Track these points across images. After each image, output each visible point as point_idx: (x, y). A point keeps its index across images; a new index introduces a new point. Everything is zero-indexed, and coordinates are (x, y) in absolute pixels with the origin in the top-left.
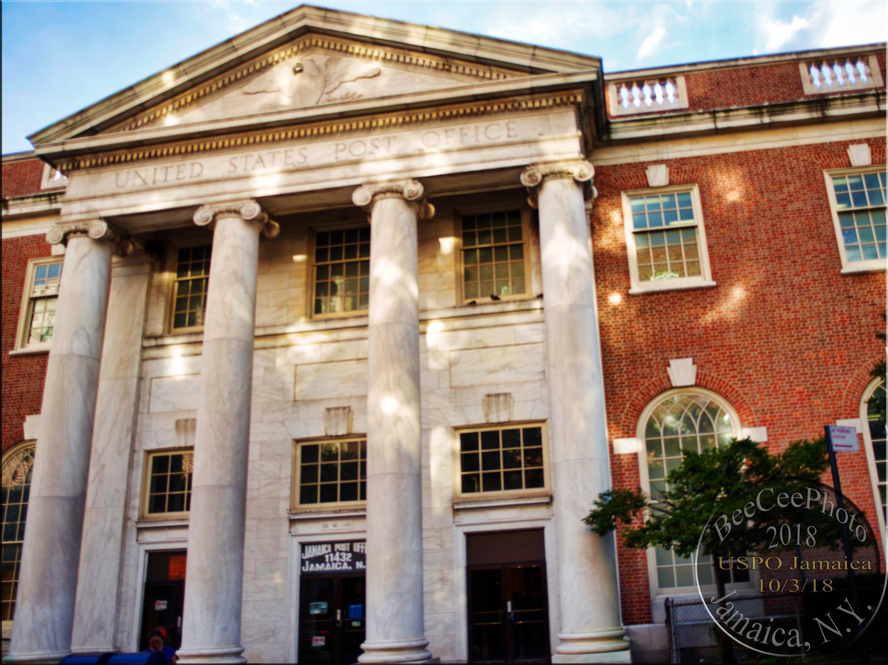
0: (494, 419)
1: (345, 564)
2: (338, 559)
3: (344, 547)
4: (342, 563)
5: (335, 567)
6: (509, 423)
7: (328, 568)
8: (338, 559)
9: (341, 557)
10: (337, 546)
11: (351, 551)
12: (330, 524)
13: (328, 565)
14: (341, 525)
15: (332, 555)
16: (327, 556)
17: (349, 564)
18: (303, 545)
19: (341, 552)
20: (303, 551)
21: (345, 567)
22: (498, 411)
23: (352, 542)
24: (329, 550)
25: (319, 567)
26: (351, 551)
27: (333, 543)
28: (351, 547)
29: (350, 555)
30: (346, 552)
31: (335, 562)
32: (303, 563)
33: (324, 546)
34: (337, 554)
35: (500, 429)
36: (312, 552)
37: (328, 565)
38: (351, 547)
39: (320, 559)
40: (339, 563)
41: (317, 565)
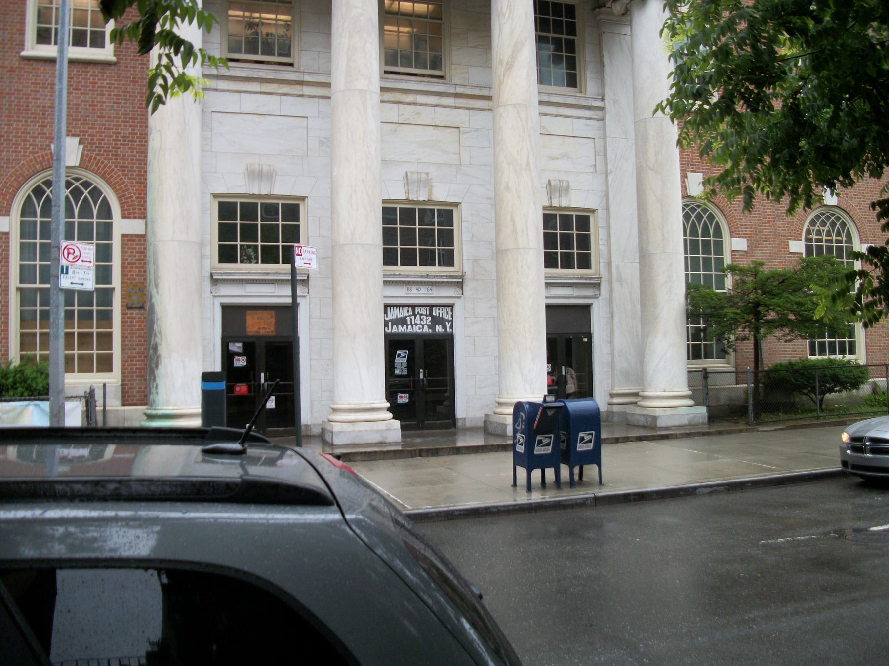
0: (555, 203)
1: (426, 327)
2: (419, 322)
3: (424, 311)
4: (423, 326)
5: (417, 329)
6: (565, 208)
7: (410, 329)
8: (419, 322)
9: (421, 320)
10: (417, 310)
11: (431, 314)
12: (414, 288)
13: (410, 326)
14: (423, 291)
15: (413, 317)
16: (408, 319)
17: (429, 327)
18: (386, 307)
19: (421, 315)
20: (386, 312)
21: (426, 329)
22: (560, 196)
23: (431, 307)
24: (411, 313)
25: (402, 329)
26: (431, 314)
27: (413, 307)
28: (431, 311)
29: (430, 318)
30: (427, 316)
31: (416, 324)
32: (386, 324)
33: (405, 309)
34: (418, 316)
35: (574, 213)
36: (394, 314)
37: (410, 326)
38: (431, 311)
39: (403, 321)
40: (420, 326)
41: (400, 326)
